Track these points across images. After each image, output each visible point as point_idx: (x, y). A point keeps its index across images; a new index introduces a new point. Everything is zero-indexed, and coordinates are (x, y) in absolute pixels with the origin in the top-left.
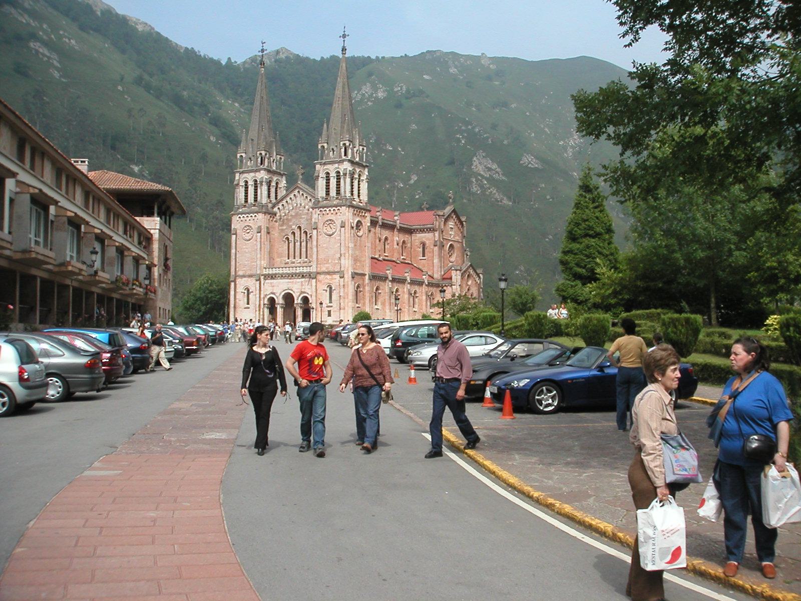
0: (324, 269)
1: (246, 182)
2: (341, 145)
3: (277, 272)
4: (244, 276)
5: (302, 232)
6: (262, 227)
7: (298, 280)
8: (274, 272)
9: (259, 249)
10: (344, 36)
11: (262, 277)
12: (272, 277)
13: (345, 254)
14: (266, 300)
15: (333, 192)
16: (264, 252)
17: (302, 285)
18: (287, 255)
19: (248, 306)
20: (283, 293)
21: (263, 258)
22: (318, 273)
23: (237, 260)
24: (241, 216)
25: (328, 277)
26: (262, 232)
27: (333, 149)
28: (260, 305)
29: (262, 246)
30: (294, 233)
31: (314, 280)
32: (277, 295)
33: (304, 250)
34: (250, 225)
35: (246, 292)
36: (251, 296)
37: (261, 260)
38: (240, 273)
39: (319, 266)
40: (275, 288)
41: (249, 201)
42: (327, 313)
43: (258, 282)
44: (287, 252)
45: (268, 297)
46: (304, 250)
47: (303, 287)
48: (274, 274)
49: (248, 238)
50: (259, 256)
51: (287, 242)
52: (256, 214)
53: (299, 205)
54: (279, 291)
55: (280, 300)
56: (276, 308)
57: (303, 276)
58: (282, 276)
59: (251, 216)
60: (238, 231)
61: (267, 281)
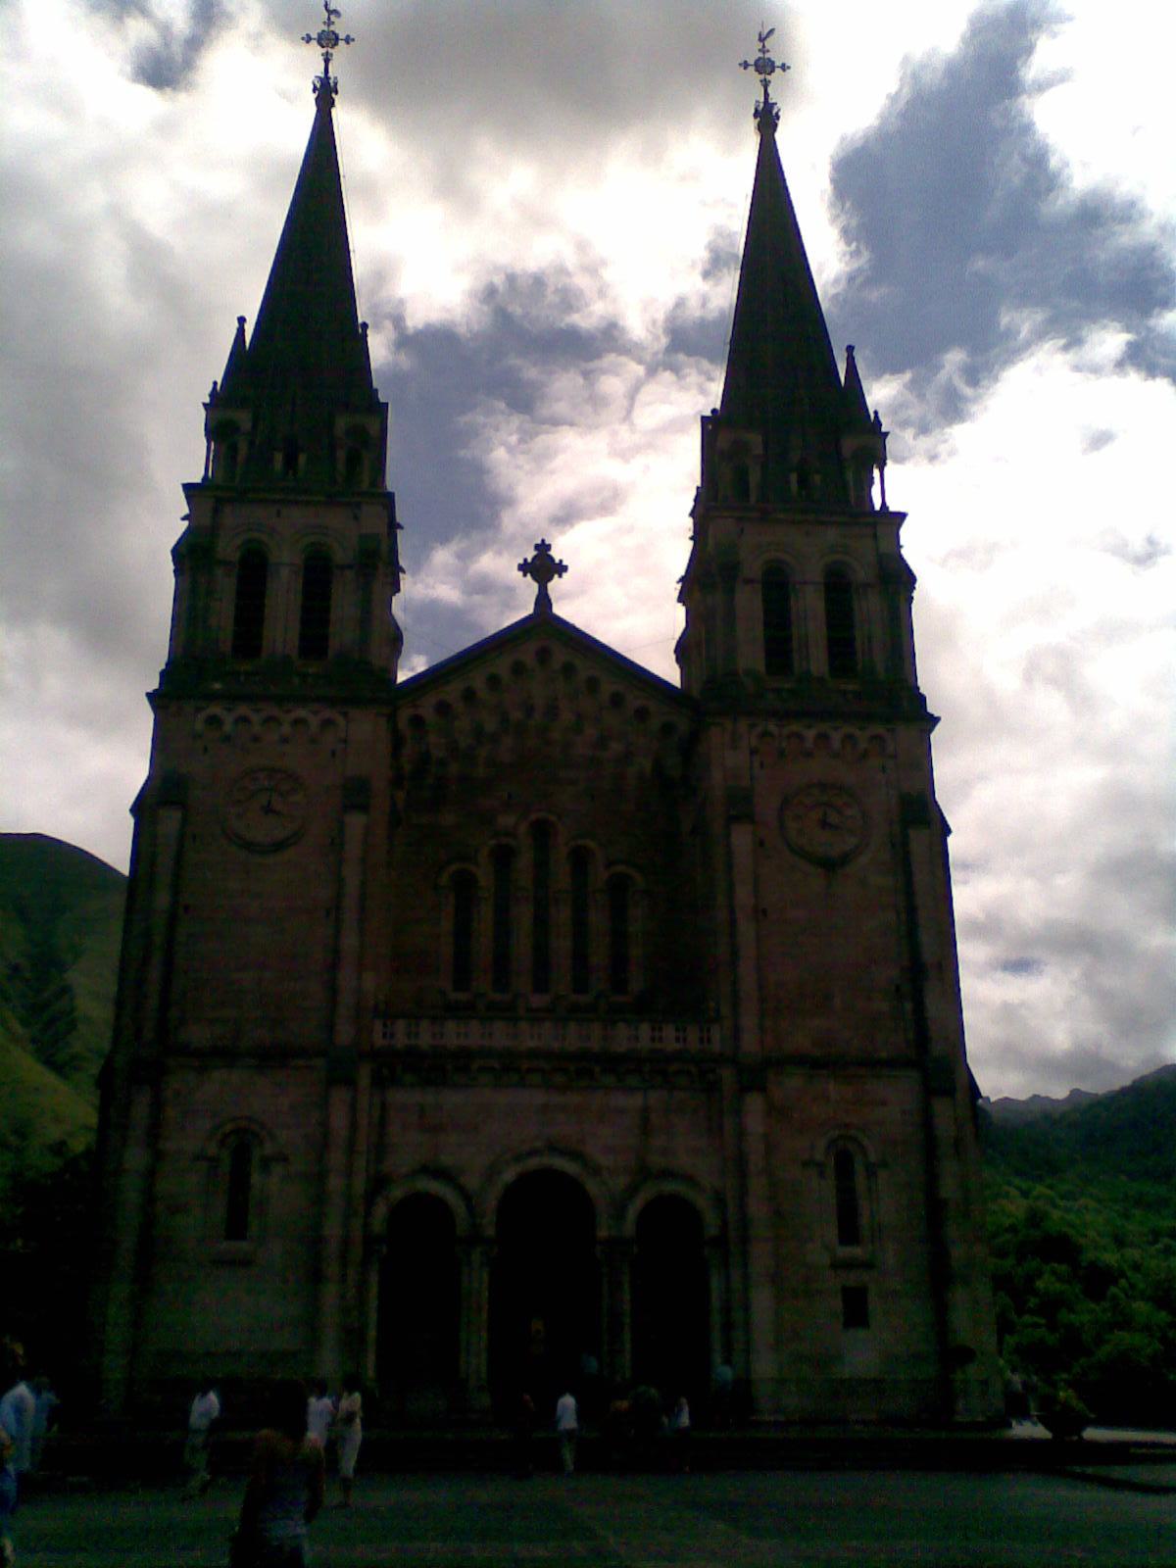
7: (620, 1100)
14: (381, 1210)
17: (646, 1128)
19: (244, 1245)
20: (509, 1175)
24: (229, 721)
25: (833, 1089)
28: (346, 1242)
31: (754, 1103)
32: (472, 1182)
33: (562, 945)
35: (226, 1157)
42: (837, 1304)
45: (397, 1193)
52: (327, 713)
57: (653, 1069)
58: (510, 1068)
59: (297, 722)
61: (397, 1096)
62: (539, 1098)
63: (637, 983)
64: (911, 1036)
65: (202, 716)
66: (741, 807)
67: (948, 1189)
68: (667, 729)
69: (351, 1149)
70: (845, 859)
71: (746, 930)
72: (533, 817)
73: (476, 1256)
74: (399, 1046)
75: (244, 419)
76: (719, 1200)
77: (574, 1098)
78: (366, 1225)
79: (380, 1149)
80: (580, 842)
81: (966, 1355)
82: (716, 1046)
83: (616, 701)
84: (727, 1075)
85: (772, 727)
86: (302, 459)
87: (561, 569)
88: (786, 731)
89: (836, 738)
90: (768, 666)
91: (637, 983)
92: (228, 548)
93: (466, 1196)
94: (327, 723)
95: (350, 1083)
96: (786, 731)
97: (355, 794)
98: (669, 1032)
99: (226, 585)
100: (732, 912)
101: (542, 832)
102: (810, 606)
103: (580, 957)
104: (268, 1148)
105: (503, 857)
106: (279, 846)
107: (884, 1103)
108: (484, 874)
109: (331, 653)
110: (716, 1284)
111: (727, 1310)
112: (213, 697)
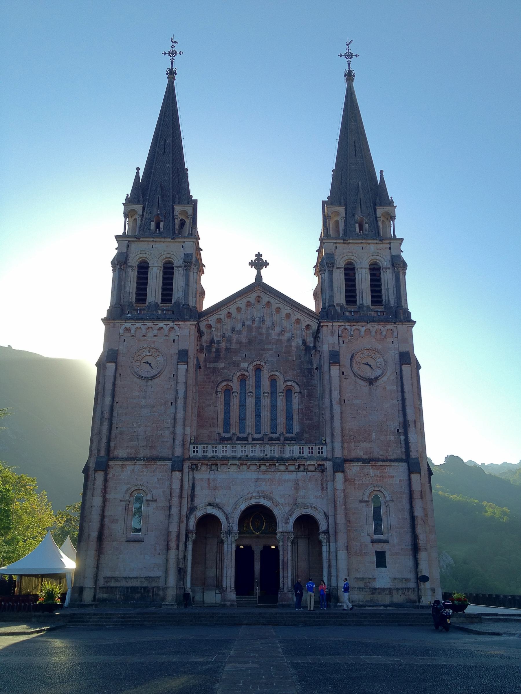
0: (360, 453)
3: (229, 454)
4: (133, 459)
9: (180, 401)
13: (415, 421)
17: (297, 488)
20: (243, 507)
22: (345, 460)
23: (114, 422)
24: (133, 328)
29: (190, 394)
31: (339, 476)
32: (228, 509)
33: (266, 414)
37: (184, 425)
38: (121, 452)
39: (345, 445)
42: (374, 558)
45: (199, 514)
46: (266, 414)
47: (302, 493)
50: (180, 415)
52: (171, 324)
59: (159, 329)
60: (120, 358)
61: (198, 476)
62: (254, 475)
63: (296, 429)
64: (404, 450)
65: (124, 326)
67: (418, 512)
68: (308, 327)
69: (181, 496)
70: (376, 378)
71: (337, 408)
72: (255, 363)
73: (230, 538)
74: (200, 456)
75: (139, 208)
76: (326, 516)
77: (268, 476)
78: (187, 526)
79: (192, 497)
80: (274, 373)
81: (425, 579)
82: (325, 455)
83: (288, 316)
84: (329, 465)
86: (162, 224)
87: (266, 264)
90: (347, 302)
91: (296, 429)
92: (134, 261)
94: (171, 329)
95: (181, 470)
96: (353, 328)
97: (183, 356)
98: (306, 449)
99: (132, 275)
100: (331, 401)
101: (258, 369)
103: (273, 419)
104: (149, 497)
105: (243, 380)
106: (153, 378)
107: (392, 477)
108: (235, 385)
109: (173, 302)
110: (325, 548)
111: (329, 561)
112: (127, 319)
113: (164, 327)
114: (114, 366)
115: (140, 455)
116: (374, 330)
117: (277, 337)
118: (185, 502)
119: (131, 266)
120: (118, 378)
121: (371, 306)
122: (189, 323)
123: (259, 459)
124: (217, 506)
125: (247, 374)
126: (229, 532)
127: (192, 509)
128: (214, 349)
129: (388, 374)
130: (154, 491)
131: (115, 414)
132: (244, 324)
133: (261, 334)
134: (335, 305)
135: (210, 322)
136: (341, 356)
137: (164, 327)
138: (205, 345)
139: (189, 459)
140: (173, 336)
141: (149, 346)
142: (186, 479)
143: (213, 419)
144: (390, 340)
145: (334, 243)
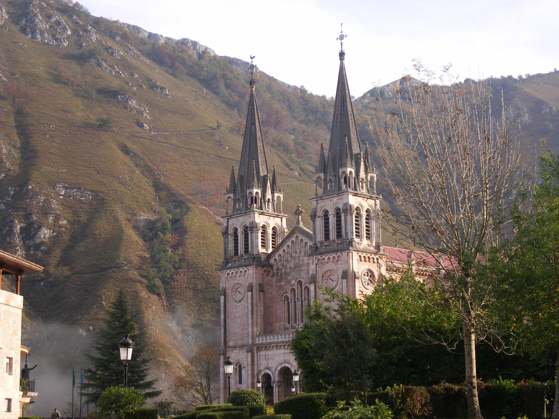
1: (236, 230)
2: (340, 174)
4: (235, 347)
5: (303, 287)
6: (254, 284)
8: (268, 341)
9: (250, 313)
10: (342, 37)
11: (255, 348)
12: (267, 347)
14: (260, 377)
15: (333, 235)
16: (257, 315)
18: (287, 319)
19: (241, 385)
20: (279, 368)
21: (255, 324)
23: (227, 327)
26: (254, 291)
27: (330, 180)
29: (255, 308)
30: (293, 290)
32: (273, 369)
34: (240, 282)
35: (238, 367)
36: (243, 372)
38: (231, 343)
40: (270, 361)
41: (239, 253)
43: (250, 354)
44: (287, 315)
45: (263, 373)
48: (268, 344)
49: (238, 299)
50: (250, 321)
51: (286, 302)
52: (246, 269)
53: (298, 254)
54: (275, 366)
55: (275, 377)
56: (272, 387)
59: (241, 272)
60: (227, 291)
66: (313, 280)
72: (298, 280)
80: (306, 285)
85: (320, 258)
88: (322, 258)
89: (331, 257)
93: (272, 373)
94: (245, 271)
97: (250, 288)
99: (231, 239)
102: (332, 220)
113: (242, 270)
114: (223, 297)
115: (238, 344)
116: (331, 257)
117: (307, 262)
118: (256, 367)
119: (230, 234)
120: (227, 303)
121: (336, 239)
122: (252, 267)
123: (284, 342)
124: (268, 368)
125: (294, 287)
126: (274, 382)
127: (259, 372)
128: (279, 274)
129: (339, 285)
130: (244, 362)
131: (227, 323)
132: (291, 257)
133: (300, 261)
134: (317, 243)
135: (276, 258)
136: (318, 276)
137: (242, 270)
138: (275, 272)
139: (256, 345)
140: (247, 274)
141: (237, 282)
142: (255, 355)
143: (281, 317)
144: (340, 262)
145: (317, 200)
